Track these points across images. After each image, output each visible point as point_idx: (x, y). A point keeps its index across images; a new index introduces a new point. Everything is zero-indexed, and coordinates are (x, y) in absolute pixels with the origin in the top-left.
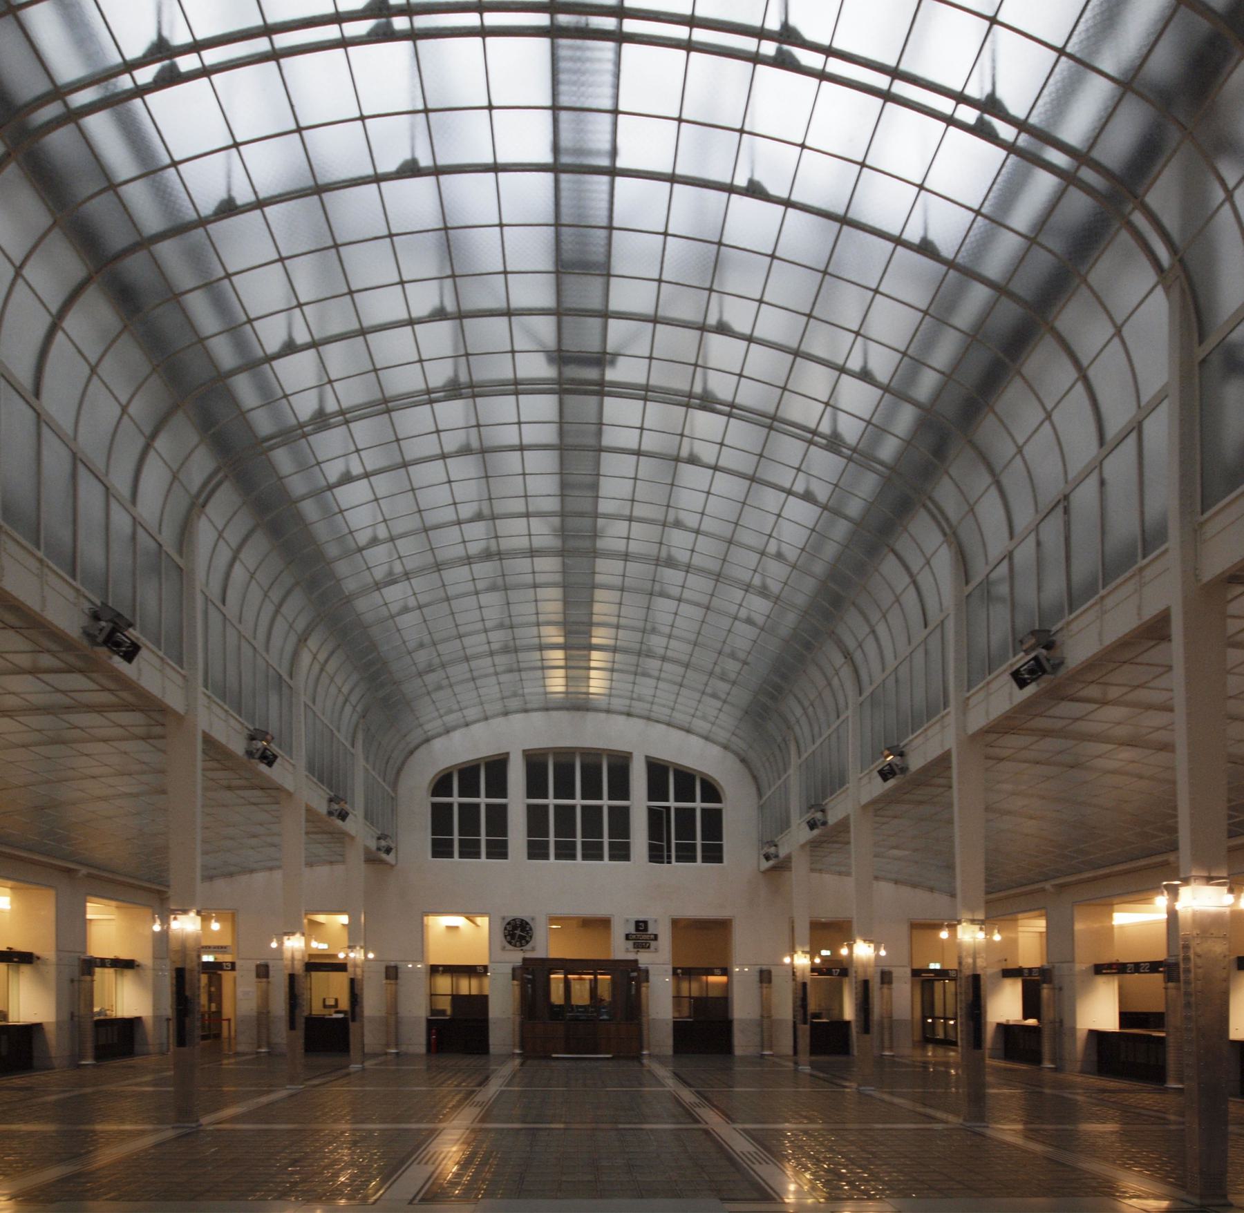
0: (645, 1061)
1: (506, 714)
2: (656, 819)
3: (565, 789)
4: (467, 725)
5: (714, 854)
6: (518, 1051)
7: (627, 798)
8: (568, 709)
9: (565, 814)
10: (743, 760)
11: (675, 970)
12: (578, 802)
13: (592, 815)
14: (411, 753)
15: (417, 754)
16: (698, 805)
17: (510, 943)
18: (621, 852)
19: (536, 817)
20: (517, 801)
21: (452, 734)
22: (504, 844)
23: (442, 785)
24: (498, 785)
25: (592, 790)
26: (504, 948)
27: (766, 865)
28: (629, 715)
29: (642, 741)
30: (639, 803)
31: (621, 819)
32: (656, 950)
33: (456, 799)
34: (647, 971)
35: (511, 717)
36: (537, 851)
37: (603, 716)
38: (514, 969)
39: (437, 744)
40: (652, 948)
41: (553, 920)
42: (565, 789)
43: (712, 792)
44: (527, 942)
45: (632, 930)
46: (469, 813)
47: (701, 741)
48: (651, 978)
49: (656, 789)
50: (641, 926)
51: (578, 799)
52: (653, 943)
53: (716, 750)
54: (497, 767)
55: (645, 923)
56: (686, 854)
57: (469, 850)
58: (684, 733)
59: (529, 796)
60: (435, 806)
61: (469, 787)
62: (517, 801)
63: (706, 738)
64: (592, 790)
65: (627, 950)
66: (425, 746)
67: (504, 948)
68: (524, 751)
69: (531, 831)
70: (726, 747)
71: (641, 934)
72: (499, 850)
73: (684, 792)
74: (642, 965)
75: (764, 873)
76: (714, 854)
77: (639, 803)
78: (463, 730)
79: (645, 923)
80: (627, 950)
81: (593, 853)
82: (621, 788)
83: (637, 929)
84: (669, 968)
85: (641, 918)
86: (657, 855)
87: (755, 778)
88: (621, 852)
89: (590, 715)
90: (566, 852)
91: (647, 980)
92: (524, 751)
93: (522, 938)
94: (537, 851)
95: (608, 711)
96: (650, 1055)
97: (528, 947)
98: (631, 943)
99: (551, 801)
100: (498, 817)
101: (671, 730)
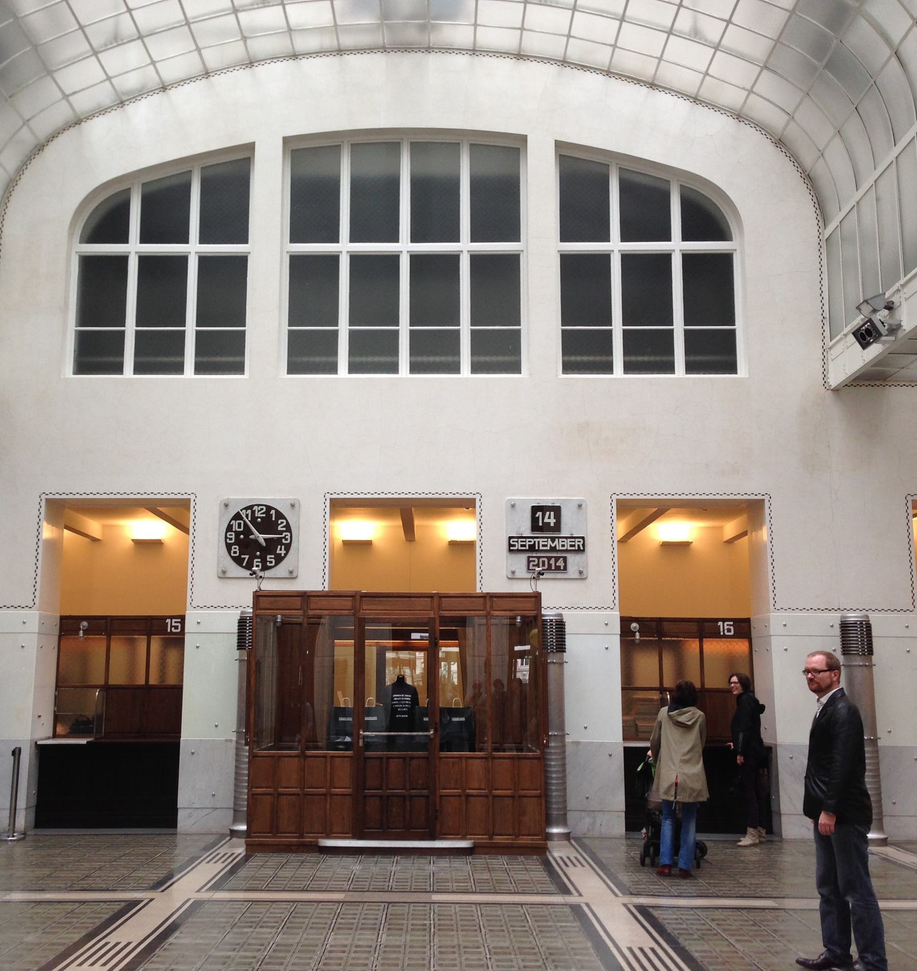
0: (558, 852)
1: (251, 63)
2: (581, 281)
3: (375, 220)
4: (164, 88)
5: (715, 353)
6: (244, 827)
7: (513, 234)
8: (384, 49)
9: (375, 273)
10: (780, 142)
11: (625, 622)
12: (404, 247)
13: (434, 273)
14: (40, 148)
15: (50, 152)
16: (677, 246)
17: (238, 561)
18: (500, 352)
19: (310, 280)
20: (268, 248)
21: (131, 108)
22: (237, 344)
23: (107, 222)
24: (228, 211)
25: (434, 219)
26: (223, 575)
27: (852, 358)
28: (520, 56)
29: (549, 112)
30: (541, 246)
31: (499, 279)
32: (582, 576)
33: (134, 248)
34: (560, 625)
35: (260, 70)
36: (309, 353)
37: (461, 61)
38: (242, 622)
39: (98, 128)
40: (572, 570)
41: (340, 506)
42: (375, 220)
43: (706, 218)
44: (279, 559)
45: (525, 529)
46: (162, 275)
47: (684, 105)
48: (569, 641)
49: (580, 210)
50: (545, 519)
51: (410, 248)
52: (572, 559)
53: (719, 123)
54: (227, 181)
55: (557, 510)
56: (649, 354)
57: (159, 356)
58: (644, 90)
59: (296, 236)
60: (89, 264)
61: (164, 218)
62: (268, 248)
63: (696, 100)
64: (434, 219)
65: (512, 577)
66: (72, 132)
67: (223, 575)
68: (286, 141)
69: (296, 314)
70: (739, 116)
71: (545, 537)
72: (223, 353)
73: (646, 218)
74: (548, 613)
75: (836, 390)
76: (715, 353)
77: (541, 246)
78: (156, 98)
79: (557, 510)
80: (512, 577)
81: (434, 355)
82: (499, 210)
83: (535, 526)
84: (615, 617)
85: (546, 499)
86: (584, 352)
87: (809, 179)
88: (500, 352)
89: (433, 60)
90: (373, 355)
91: (561, 647)
92: (286, 141)
93: (272, 545)
94: (309, 353)
95: (474, 51)
96: (567, 837)
97: (281, 570)
98: (523, 558)
99: (345, 247)
100: (226, 282)
101: (615, 84)
